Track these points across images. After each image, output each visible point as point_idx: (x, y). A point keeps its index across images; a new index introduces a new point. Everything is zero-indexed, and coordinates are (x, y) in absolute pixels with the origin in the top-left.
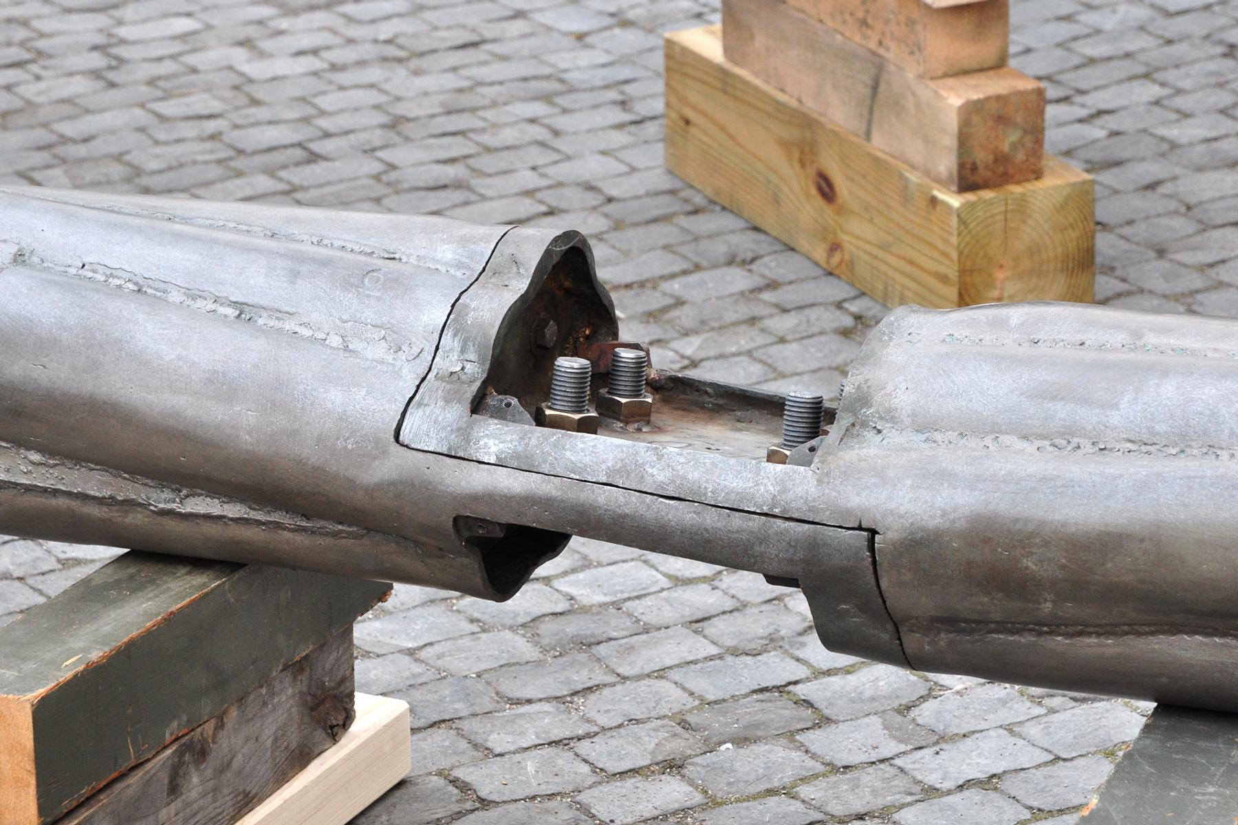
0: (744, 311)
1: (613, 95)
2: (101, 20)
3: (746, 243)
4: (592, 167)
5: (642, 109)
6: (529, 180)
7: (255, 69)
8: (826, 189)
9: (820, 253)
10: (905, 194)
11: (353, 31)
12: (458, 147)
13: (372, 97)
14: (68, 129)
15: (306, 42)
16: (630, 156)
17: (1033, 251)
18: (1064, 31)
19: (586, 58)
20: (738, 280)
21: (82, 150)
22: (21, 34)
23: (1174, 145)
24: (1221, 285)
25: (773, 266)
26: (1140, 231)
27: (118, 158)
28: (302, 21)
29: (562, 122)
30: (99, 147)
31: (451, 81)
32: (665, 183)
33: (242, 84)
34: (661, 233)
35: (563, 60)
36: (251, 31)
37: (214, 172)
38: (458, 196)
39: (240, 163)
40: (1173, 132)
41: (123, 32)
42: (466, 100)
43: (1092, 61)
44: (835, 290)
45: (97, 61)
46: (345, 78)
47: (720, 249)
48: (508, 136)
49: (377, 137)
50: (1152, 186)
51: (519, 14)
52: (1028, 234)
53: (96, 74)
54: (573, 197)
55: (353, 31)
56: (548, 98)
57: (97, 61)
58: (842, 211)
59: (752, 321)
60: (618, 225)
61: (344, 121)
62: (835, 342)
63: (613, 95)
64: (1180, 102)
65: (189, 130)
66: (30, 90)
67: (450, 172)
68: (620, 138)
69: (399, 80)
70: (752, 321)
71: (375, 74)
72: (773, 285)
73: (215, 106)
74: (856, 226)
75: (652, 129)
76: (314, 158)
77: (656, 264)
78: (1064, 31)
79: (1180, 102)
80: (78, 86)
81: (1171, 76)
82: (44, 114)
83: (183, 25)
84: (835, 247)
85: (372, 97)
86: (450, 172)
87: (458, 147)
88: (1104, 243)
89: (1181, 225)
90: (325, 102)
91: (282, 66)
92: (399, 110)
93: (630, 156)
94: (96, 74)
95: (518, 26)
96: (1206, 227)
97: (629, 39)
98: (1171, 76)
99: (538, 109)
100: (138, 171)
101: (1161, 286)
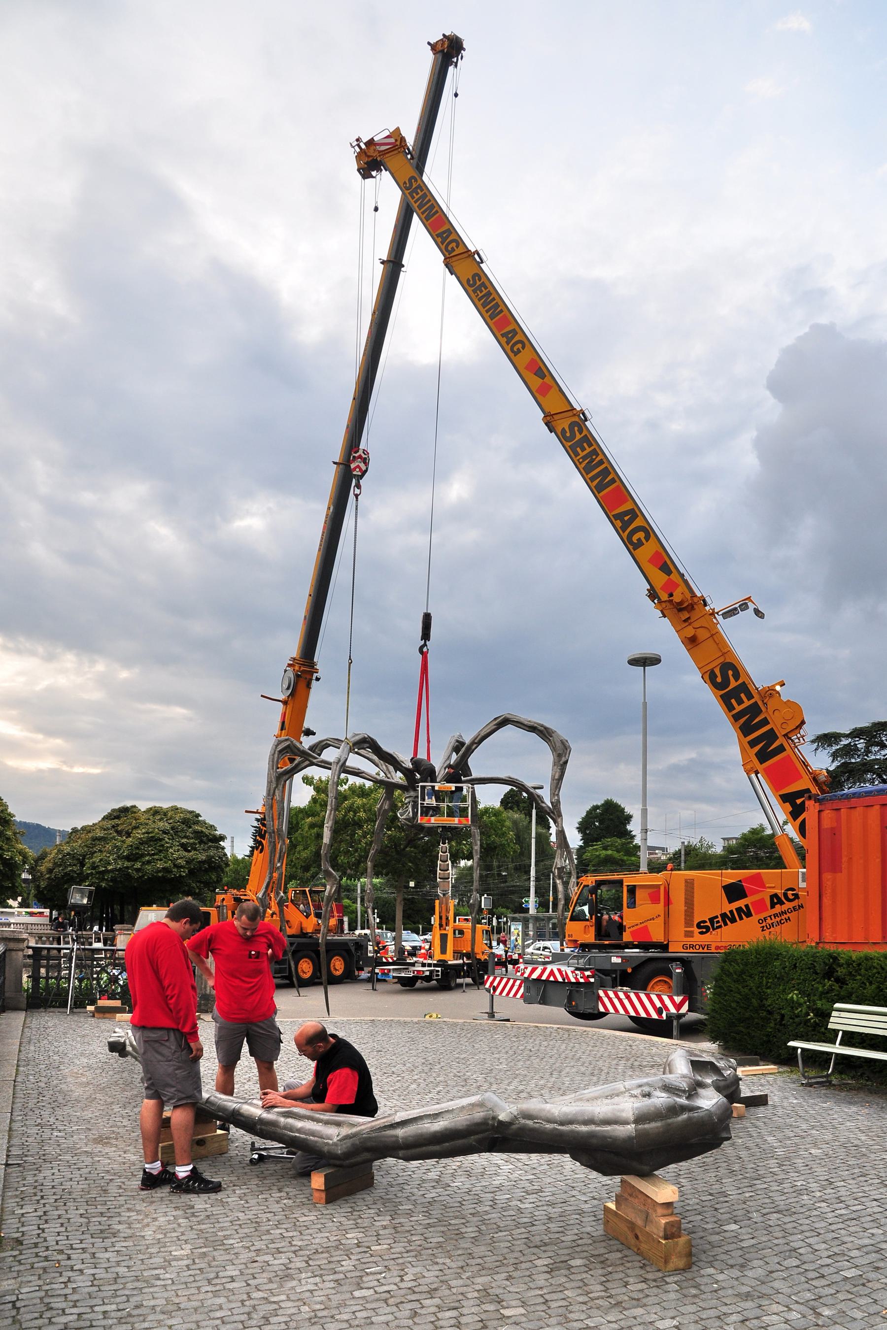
0: (621, 1262)
1: (593, 1214)
2: (492, 1195)
3: (620, 1247)
4: (589, 1229)
5: (599, 1217)
6: (576, 1231)
7: (522, 1206)
8: (637, 1237)
9: (636, 1250)
10: (653, 1238)
11: (541, 1199)
12: (562, 1224)
13: (544, 1213)
14: (485, 1217)
15: (531, 1201)
16: (596, 1227)
17: (679, 1253)
18: (682, 1204)
19: (587, 1206)
20: (619, 1255)
21: (488, 1222)
22: (477, 1197)
23: (706, 1229)
24: (717, 1260)
25: (626, 1252)
26: (700, 1247)
27: (495, 1224)
28: (531, 1196)
29: (582, 1219)
30: (492, 1221)
31: (560, 1210)
32: (603, 1233)
33: (519, 1209)
34: (603, 1244)
35: (583, 1206)
36: (521, 1198)
37: (514, 1228)
38: (562, 1234)
39: (519, 1226)
40: (705, 1226)
41: (496, 1197)
42: (563, 1214)
43: (688, 1210)
44: (639, 1258)
45: (491, 1203)
46: (540, 1208)
47: (615, 1248)
48: (572, 1222)
49: (546, 1221)
50: (702, 1238)
51: (574, 1196)
52: (678, 1249)
53: (491, 1206)
54: (585, 1236)
55: (541, 1199)
56: (579, 1214)
57: (491, 1203)
58: (640, 1242)
59: (622, 1264)
60: (594, 1242)
61: (539, 1218)
62: (639, 1269)
63: (593, 1214)
64: (706, 1220)
65: (509, 1218)
66: (478, 1209)
67: (561, 1229)
68: (594, 1223)
69: (550, 1209)
70: (622, 1264)
71: (545, 1208)
72: (626, 1256)
73: (514, 1213)
74: (642, 1245)
75: (600, 1221)
76: (534, 1225)
77: (603, 1251)
78: (682, 1204)
79: (706, 1220)
80: (488, 1208)
81: (704, 1214)
82: (481, 1214)
83: (508, 1196)
84: (639, 1249)
85: (544, 1213)
86: (561, 1229)
87: (562, 1224)
88: (693, 1249)
89: (708, 1246)
90: (536, 1213)
91: (527, 1206)
92: (550, 1216)
93: (596, 1227)
94: (491, 1206)
95: (573, 1199)
96: (713, 1247)
97: (596, 1202)
98: (704, 1214)
99: (578, 1216)
100: (499, 1227)
101: (705, 1260)
